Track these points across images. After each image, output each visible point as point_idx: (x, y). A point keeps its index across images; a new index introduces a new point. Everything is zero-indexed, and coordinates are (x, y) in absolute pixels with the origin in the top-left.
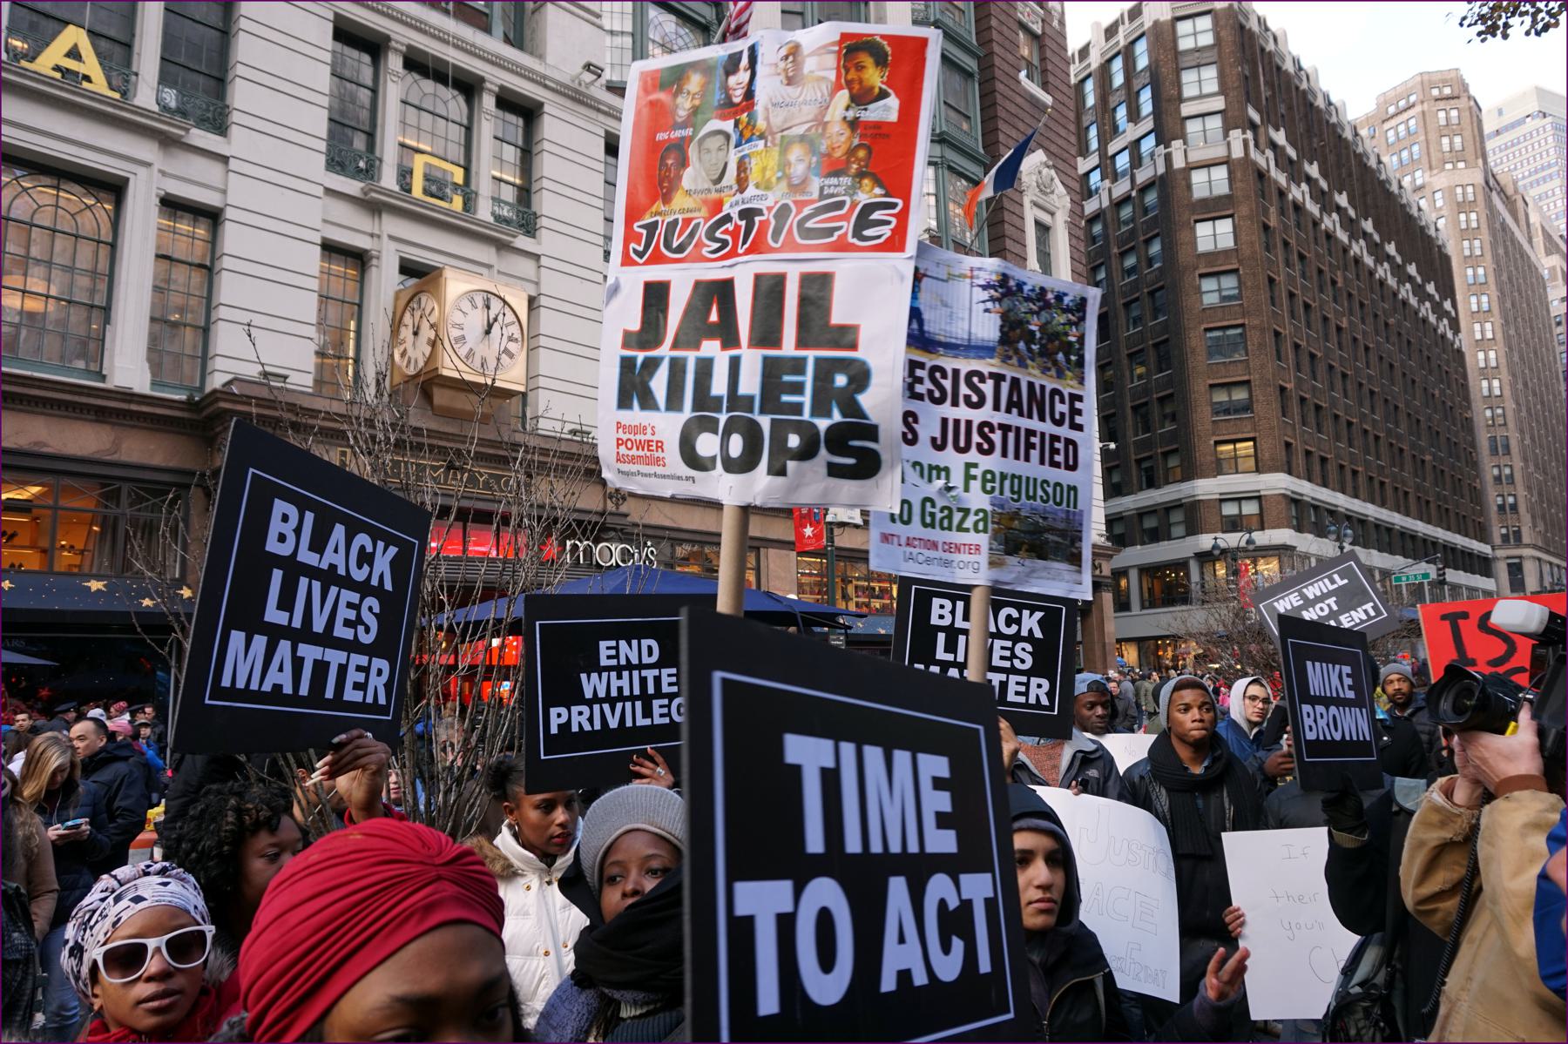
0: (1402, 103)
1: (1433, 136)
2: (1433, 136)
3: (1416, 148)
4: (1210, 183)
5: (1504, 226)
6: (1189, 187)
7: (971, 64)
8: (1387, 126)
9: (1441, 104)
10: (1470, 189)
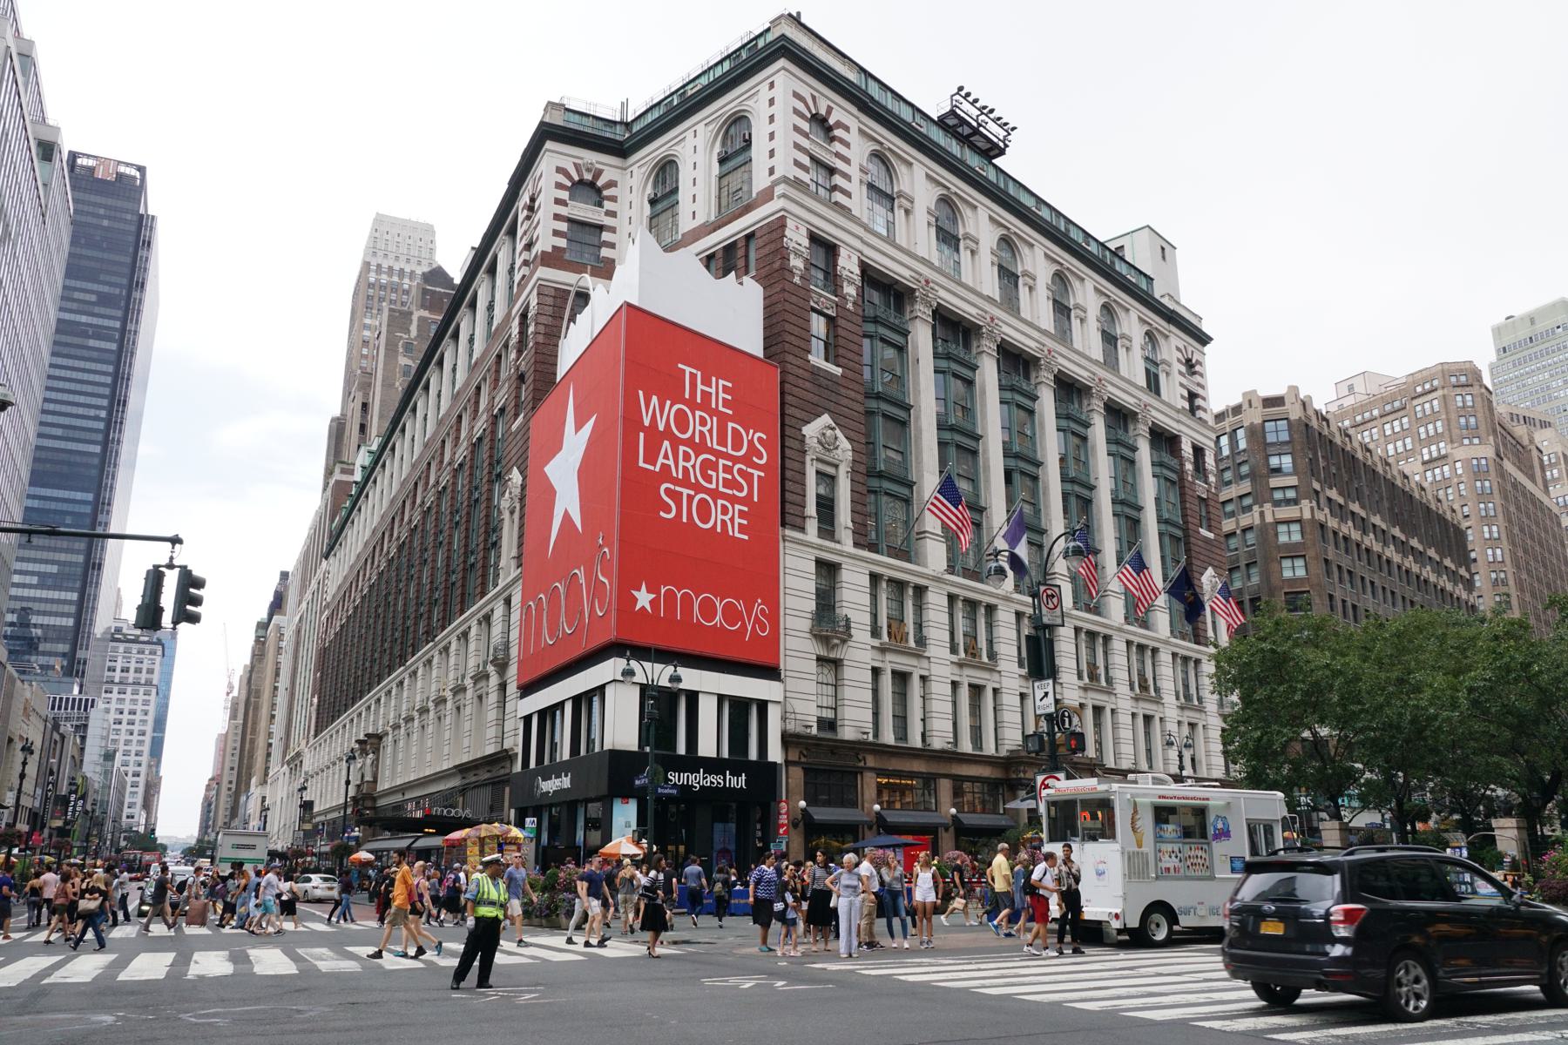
0: (1427, 386)
1: (1453, 416)
2: (1453, 416)
3: (1439, 424)
4: (1290, 536)
5: (1516, 485)
6: (1276, 535)
7: (1179, 533)
8: (1415, 402)
9: (1459, 391)
10: (1483, 462)
